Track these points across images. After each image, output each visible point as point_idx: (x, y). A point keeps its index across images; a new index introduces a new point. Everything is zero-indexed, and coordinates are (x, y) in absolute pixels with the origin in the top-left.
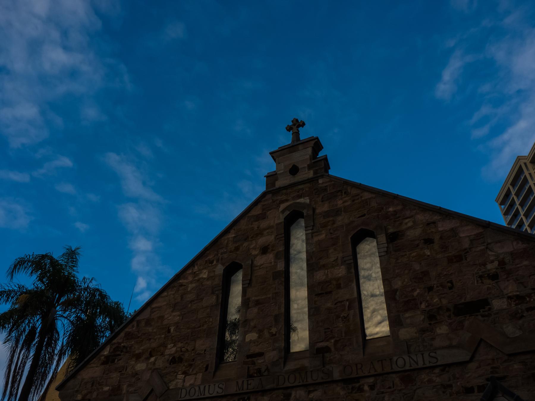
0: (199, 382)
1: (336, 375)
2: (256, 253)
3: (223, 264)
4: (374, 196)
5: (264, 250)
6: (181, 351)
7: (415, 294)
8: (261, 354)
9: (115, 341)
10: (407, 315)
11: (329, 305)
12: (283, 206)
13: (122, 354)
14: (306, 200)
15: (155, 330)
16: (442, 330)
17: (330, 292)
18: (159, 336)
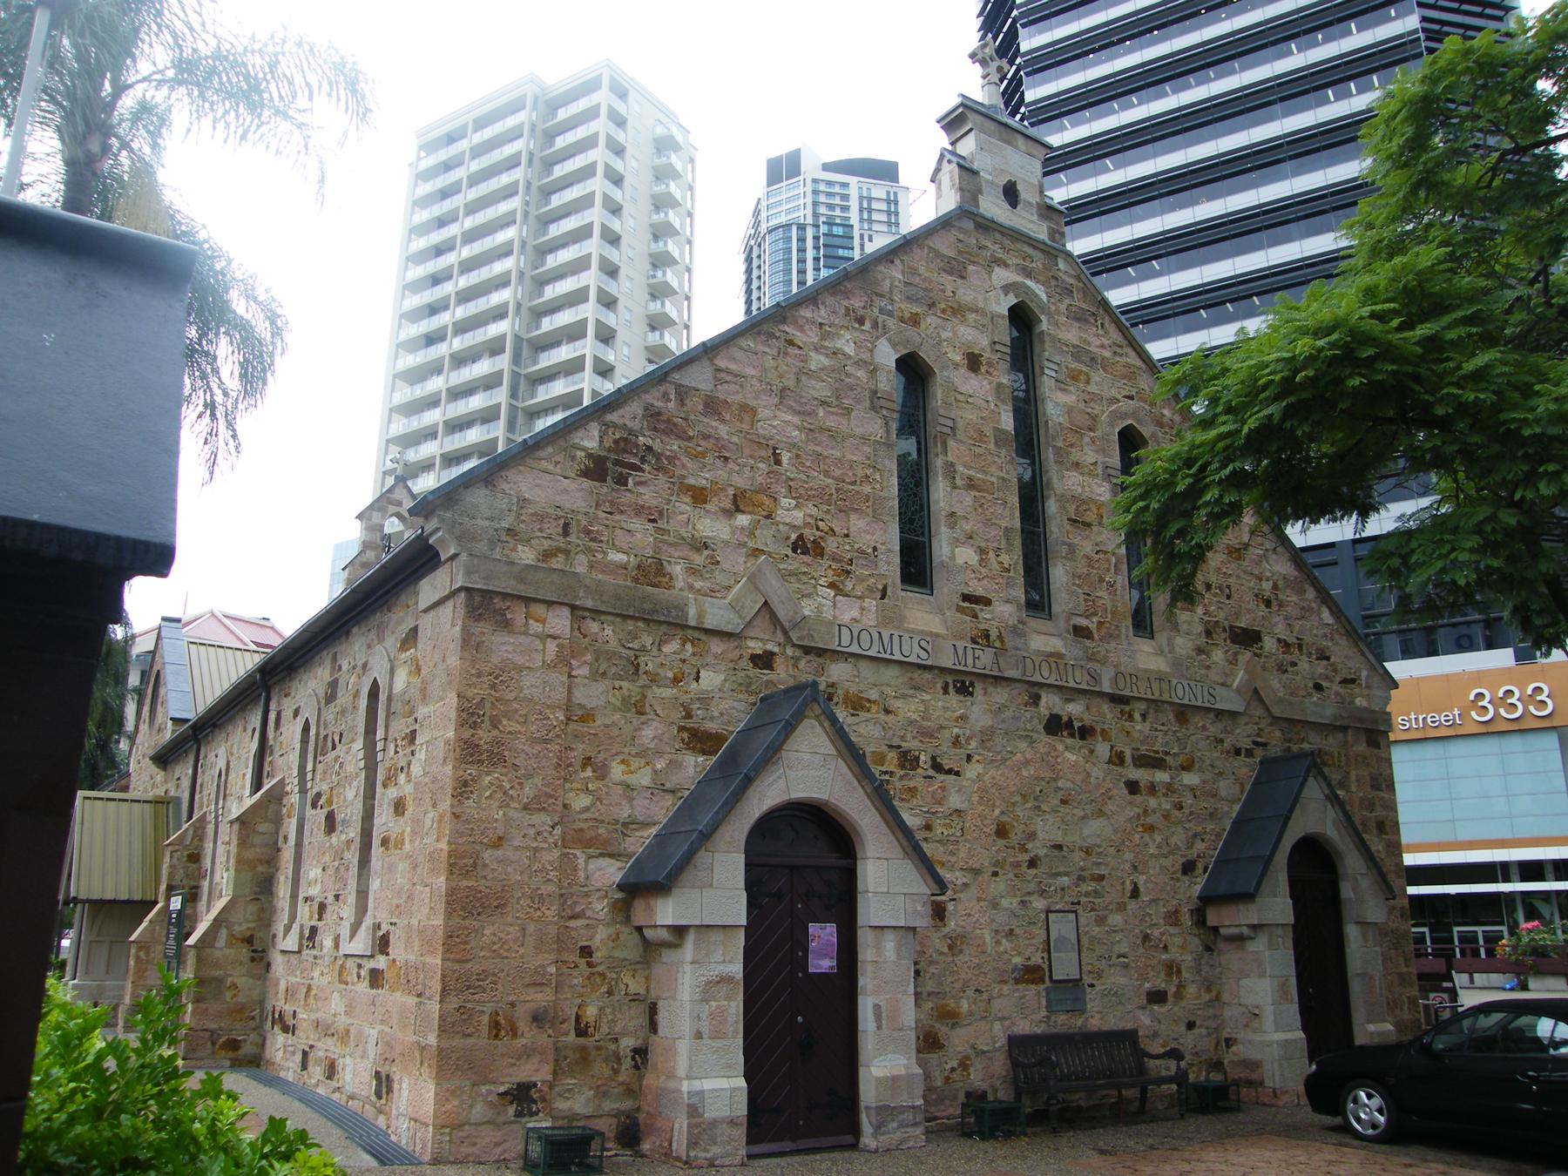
0: (870, 620)
2: (958, 358)
3: (894, 346)
5: (974, 362)
8: (987, 602)
9: (612, 417)
12: (1002, 276)
13: (645, 467)
14: (1040, 291)
15: (735, 439)
16: (1218, 656)
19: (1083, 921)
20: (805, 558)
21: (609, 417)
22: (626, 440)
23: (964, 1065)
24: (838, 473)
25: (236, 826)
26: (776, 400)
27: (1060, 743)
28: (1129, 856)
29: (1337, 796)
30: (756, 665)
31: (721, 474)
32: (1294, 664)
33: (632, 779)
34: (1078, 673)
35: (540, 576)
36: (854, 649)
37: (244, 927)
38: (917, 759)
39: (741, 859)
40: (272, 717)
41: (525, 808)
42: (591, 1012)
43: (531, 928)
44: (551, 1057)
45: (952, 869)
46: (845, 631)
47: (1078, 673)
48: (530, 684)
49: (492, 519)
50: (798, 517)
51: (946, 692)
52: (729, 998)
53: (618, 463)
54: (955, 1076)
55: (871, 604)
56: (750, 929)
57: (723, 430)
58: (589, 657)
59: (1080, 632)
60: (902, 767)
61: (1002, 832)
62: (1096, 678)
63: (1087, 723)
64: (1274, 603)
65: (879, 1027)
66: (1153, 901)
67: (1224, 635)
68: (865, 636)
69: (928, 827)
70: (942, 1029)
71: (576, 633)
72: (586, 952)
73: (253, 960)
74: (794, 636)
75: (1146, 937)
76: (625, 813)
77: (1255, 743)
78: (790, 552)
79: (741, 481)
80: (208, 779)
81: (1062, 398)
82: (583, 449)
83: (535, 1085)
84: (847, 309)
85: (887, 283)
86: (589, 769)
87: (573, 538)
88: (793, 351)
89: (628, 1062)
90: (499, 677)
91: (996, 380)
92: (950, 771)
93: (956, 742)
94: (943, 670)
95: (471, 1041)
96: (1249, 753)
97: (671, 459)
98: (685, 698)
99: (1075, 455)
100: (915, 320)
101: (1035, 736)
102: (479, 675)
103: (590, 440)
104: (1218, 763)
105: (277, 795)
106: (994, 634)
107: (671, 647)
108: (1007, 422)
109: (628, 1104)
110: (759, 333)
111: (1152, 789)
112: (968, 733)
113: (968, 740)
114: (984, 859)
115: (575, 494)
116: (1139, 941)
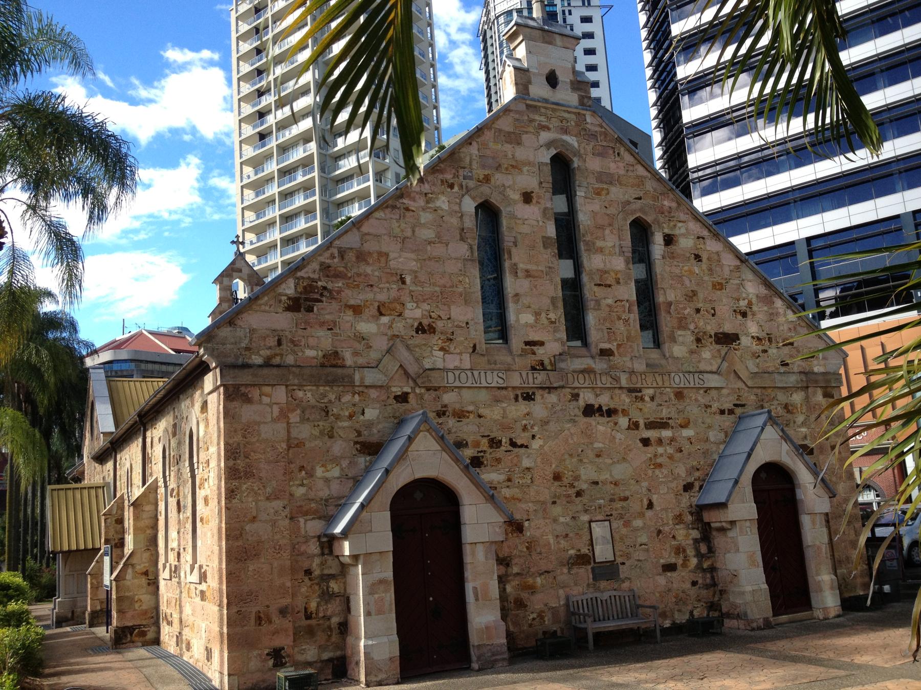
1: (624, 382)
3: (473, 199)
4: (649, 175)
5: (527, 198)
6: (431, 317)
7: (686, 312)
8: (541, 344)
10: (680, 332)
11: (610, 301)
12: (545, 136)
13: (324, 299)
14: (572, 140)
16: (706, 354)
17: (610, 286)
18: (387, 285)
19: (614, 525)
20: (424, 336)
21: (299, 274)
22: (310, 286)
23: (541, 616)
24: (442, 282)
25: (131, 508)
26: (399, 245)
27: (592, 421)
28: (645, 484)
29: (788, 436)
30: (398, 401)
31: (370, 296)
32: (765, 351)
33: (328, 475)
34: (604, 378)
35: (266, 371)
36: (457, 384)
37: (142, 565)
38: (500, 441)
39: (388, 514)
40: (148, 440)
41: (268, 499)
42: (313, 605)
43: (275, 564)
44: (291, 633)
45: (526, 502)
46: (450, 374)
47: (604, 378)
48: (266, 431)
49: (236, 343)
50: (418, 313)
51: (516, 399)
52: (386, 591)
53: (306, 299)
54: (535, 622)
55: (466, 357)
56: (395, 553)
57: (369, 270)
58: (298, 411)
59: (605, 353)
60: (491, 447)
61: (557, 477)
62: (617, 380)
63: (612, 406)
64: (749, 313)
65: (477, 600)
66: (662, 510)
67: (710, 340)
68: (463, 375)
69: (509, 480)
70: (524, 595)
71: (290, 399)
72: (308, 572)
73: (149, 584)
74: (419, 381)
75: (659, 532)
76: (328, 493)
77: (735, 405)
78: (414, 333)
79: (382, 297)
80: (122, 472)
81: (589, 207)
82: (286, 295)
83: (283, 648)
84: (442, 181)
85: (468, 159)
86: (304, 472)
87: (284, 347)
88: (408, 214)
89: (336, 631)
90: (248, 430)
91: (543, 206)
92: (522, 446)
93: (525, 428)
94: (514, 388)
95: (246, 628)
96: (731, 412)
97: (339, 292)
98: (357, 426)
99: (599, 244)
100: (487, 179)
101: (577, 419)
102: (235, 431)
103: (289, 289)
104: (708, 421)
105: (154, 488)
106: (547, 362)
107: (347, 398)
108: (551, 230)
109: (339, 653)
110: (387, 207)
111: (660, 441)
112: (532, 422)
113: (532, 427)
114: (546, 495)
115: (283, 321)
116: (655, 535)
